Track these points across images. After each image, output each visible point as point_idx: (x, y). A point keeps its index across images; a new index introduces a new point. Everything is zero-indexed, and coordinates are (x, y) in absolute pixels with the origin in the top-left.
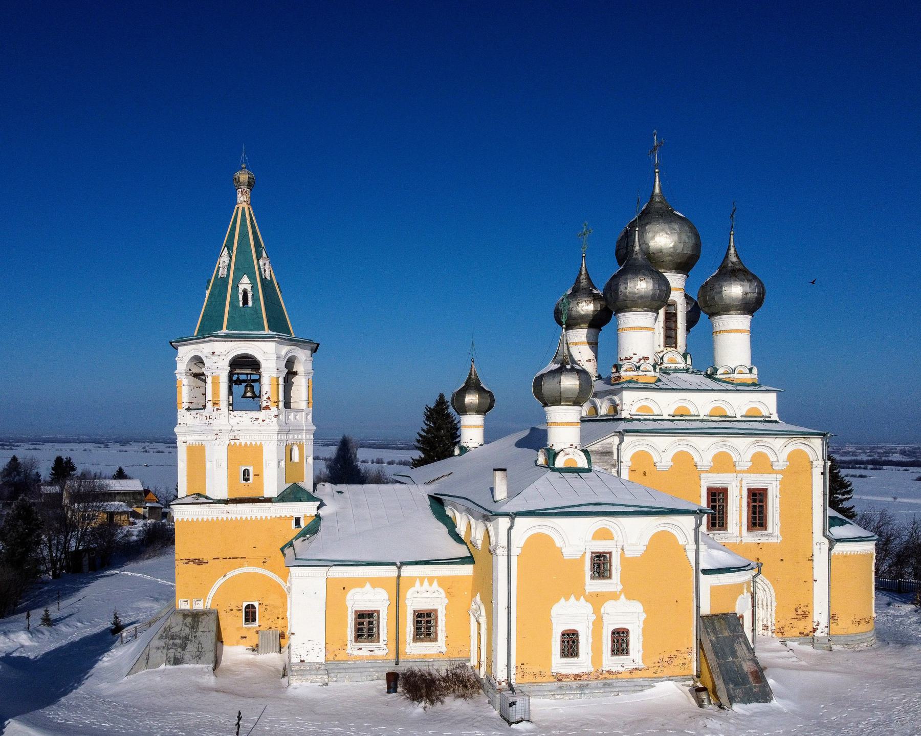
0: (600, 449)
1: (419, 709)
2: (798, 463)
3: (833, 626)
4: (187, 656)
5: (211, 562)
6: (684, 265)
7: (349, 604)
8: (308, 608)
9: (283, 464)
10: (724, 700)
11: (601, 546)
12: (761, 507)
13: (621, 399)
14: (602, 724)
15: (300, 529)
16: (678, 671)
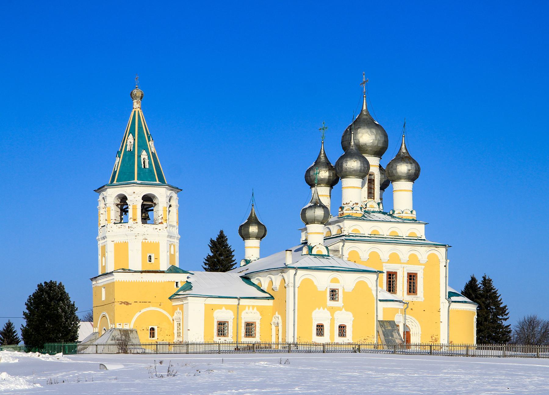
5: (133, 304)
11: (334, 286)
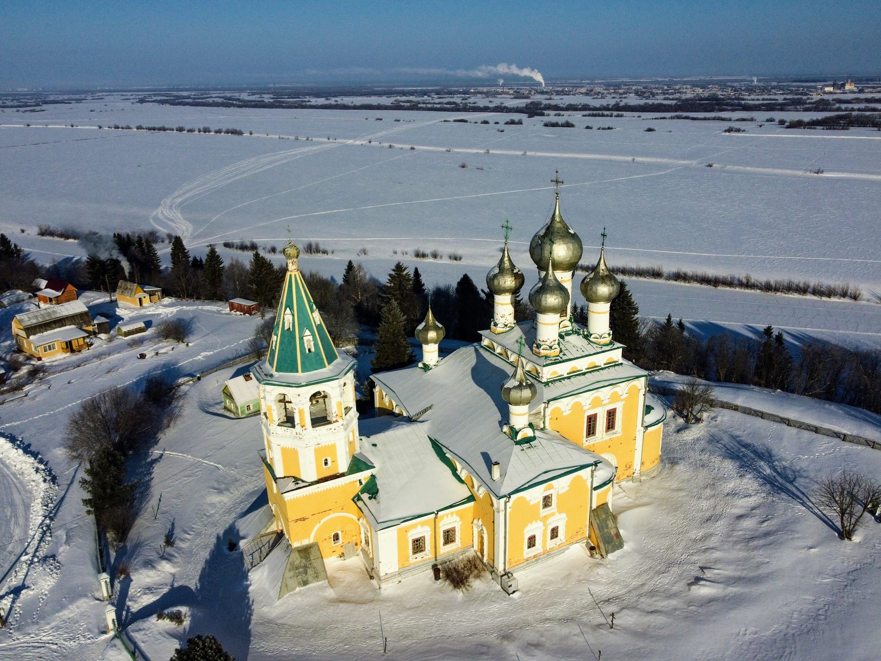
4: (310, 579)
5: (311, 518)
10: (604, 553)
16: (580, 537)
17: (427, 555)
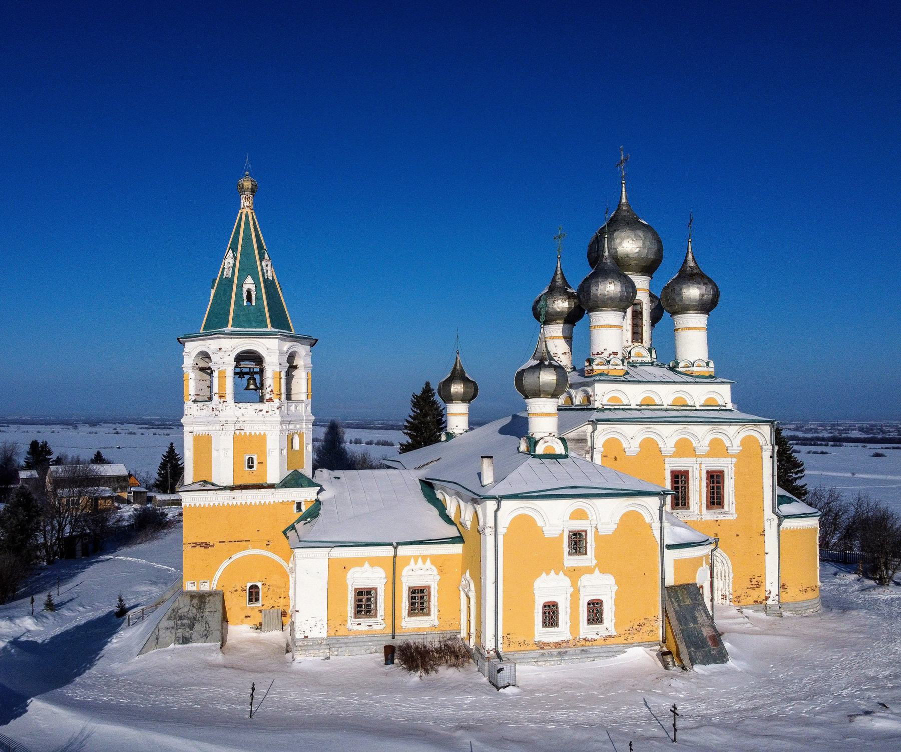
0: (576, 437)
1: (415, 678)
2: (750, 448)
3: (783, 594)
5: (217, 545)
6: (648, 268)
7: (349, 582)
8: (311, 587)
9: (285, 452)
11: (577, 525)
12: (718, 487)
13: (594, 391)
14: (580, 687)
15: (301, 513)
16: (646, 637)
17: (379, 624)
